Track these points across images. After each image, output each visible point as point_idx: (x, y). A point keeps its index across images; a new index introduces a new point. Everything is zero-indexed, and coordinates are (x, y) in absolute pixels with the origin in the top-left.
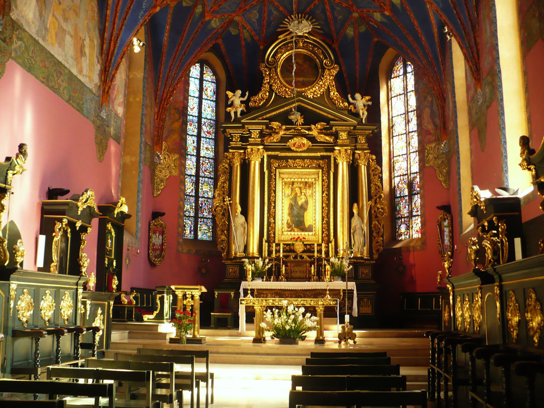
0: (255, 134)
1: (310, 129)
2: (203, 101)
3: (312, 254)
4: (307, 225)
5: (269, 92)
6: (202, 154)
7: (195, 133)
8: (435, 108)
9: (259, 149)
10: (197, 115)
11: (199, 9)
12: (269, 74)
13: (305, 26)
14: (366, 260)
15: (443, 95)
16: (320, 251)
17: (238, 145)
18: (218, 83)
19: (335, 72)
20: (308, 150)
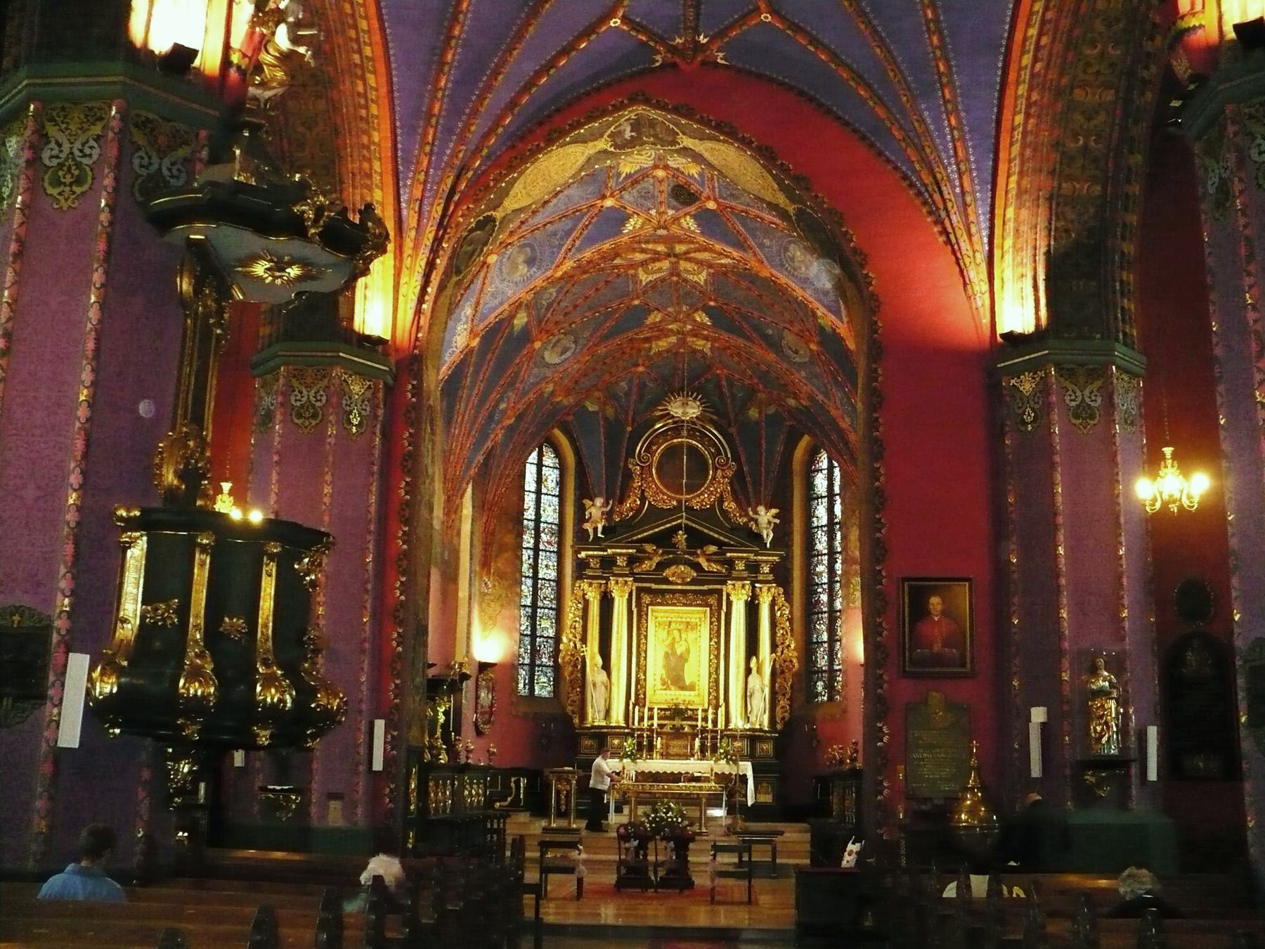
0: (621, 561)
1: (694, 554)
3: (694, 723)
4: (688, 682)
6: (540, 576)
7: (531, 545)
9: (626, 582)
10: (533, 517)
14: (765, 732)
16: (705, 719)
18: (562, 469)
20: (693, 582)
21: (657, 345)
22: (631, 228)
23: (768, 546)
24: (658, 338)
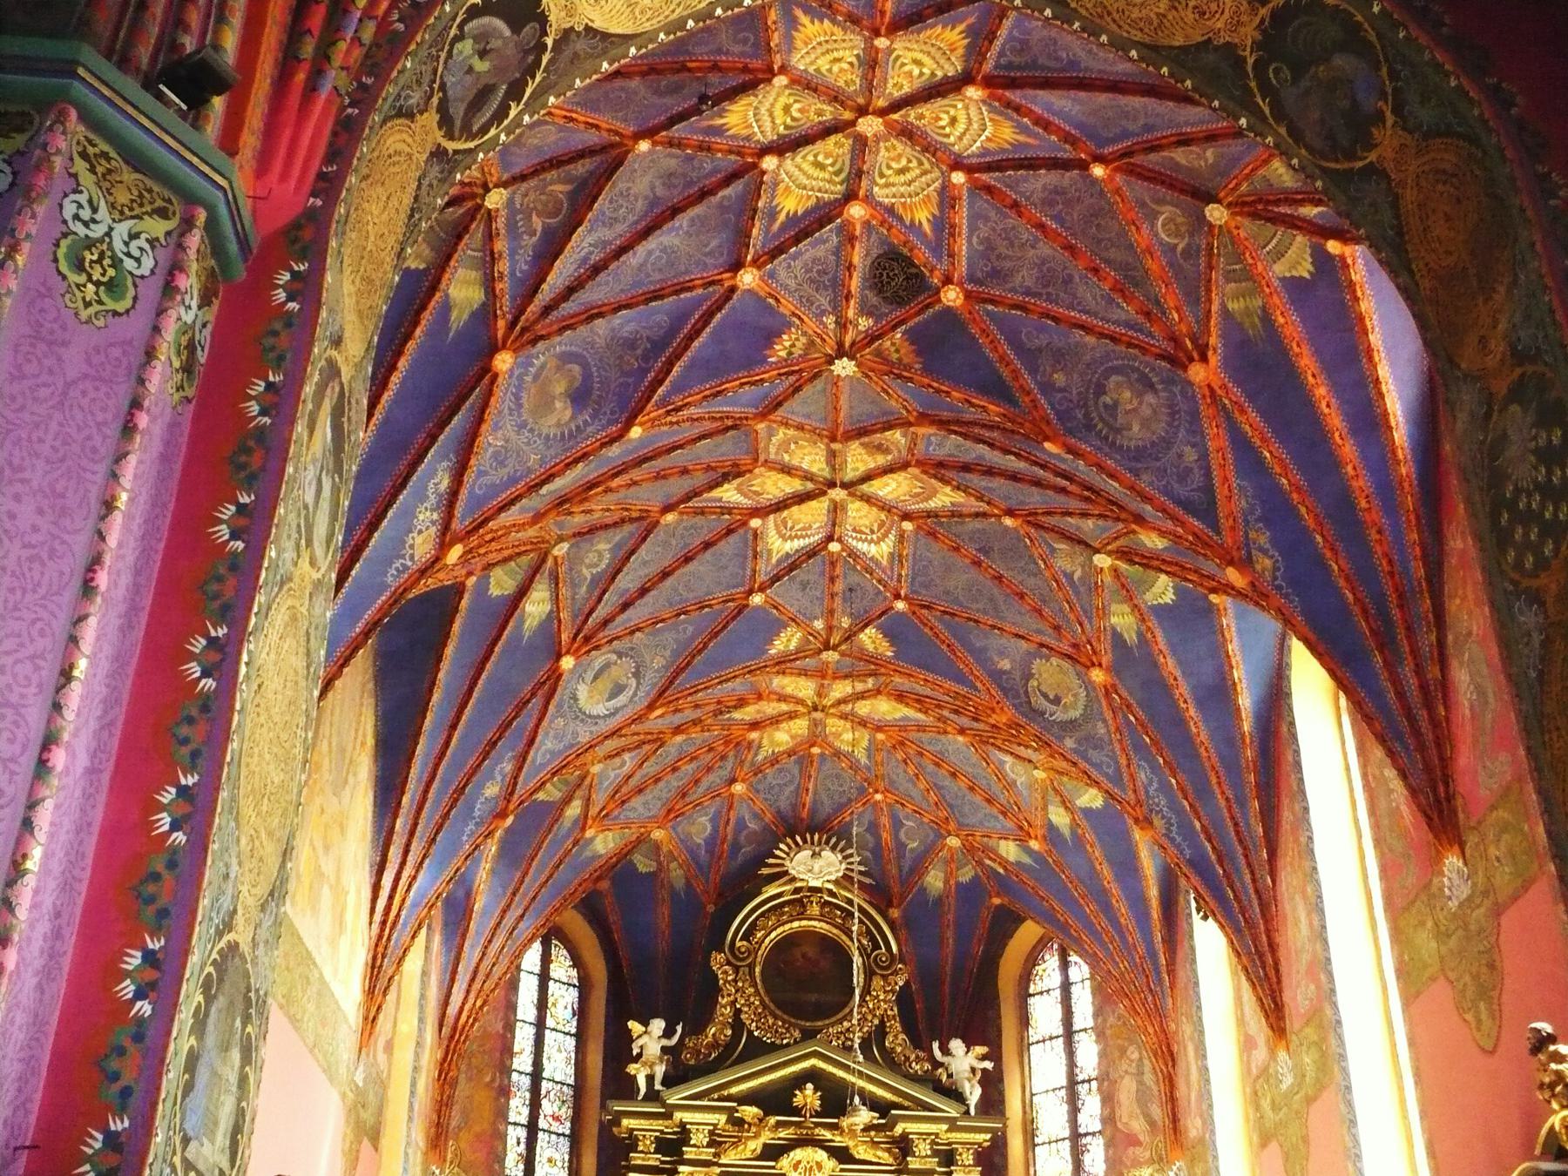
0: (699, 1138)
2: (547, 1032)
5: (733, 1027)
7: (523, 1119)
8: (1149, 1078)
10: (529, 1069)
11: (574, 810)
12: (735, 981)
13: (829, 865)
15: (1168, 1046)
17: (651, 1163)
18: (584, 987)
19: (901, 983)
21: (772, 742)
22: (783, 354)
23: (972, 1112)
24: (775, 721)
